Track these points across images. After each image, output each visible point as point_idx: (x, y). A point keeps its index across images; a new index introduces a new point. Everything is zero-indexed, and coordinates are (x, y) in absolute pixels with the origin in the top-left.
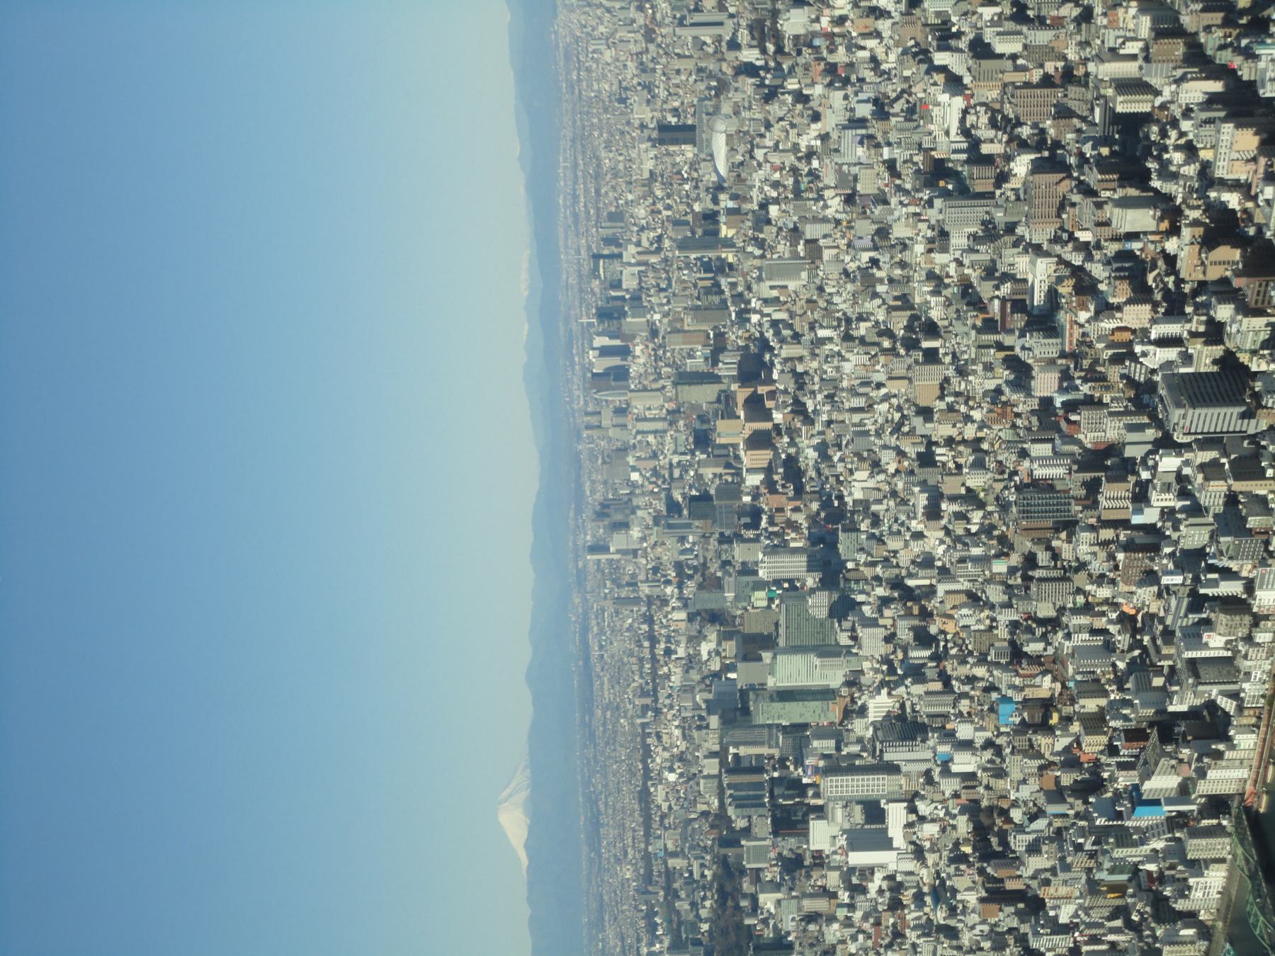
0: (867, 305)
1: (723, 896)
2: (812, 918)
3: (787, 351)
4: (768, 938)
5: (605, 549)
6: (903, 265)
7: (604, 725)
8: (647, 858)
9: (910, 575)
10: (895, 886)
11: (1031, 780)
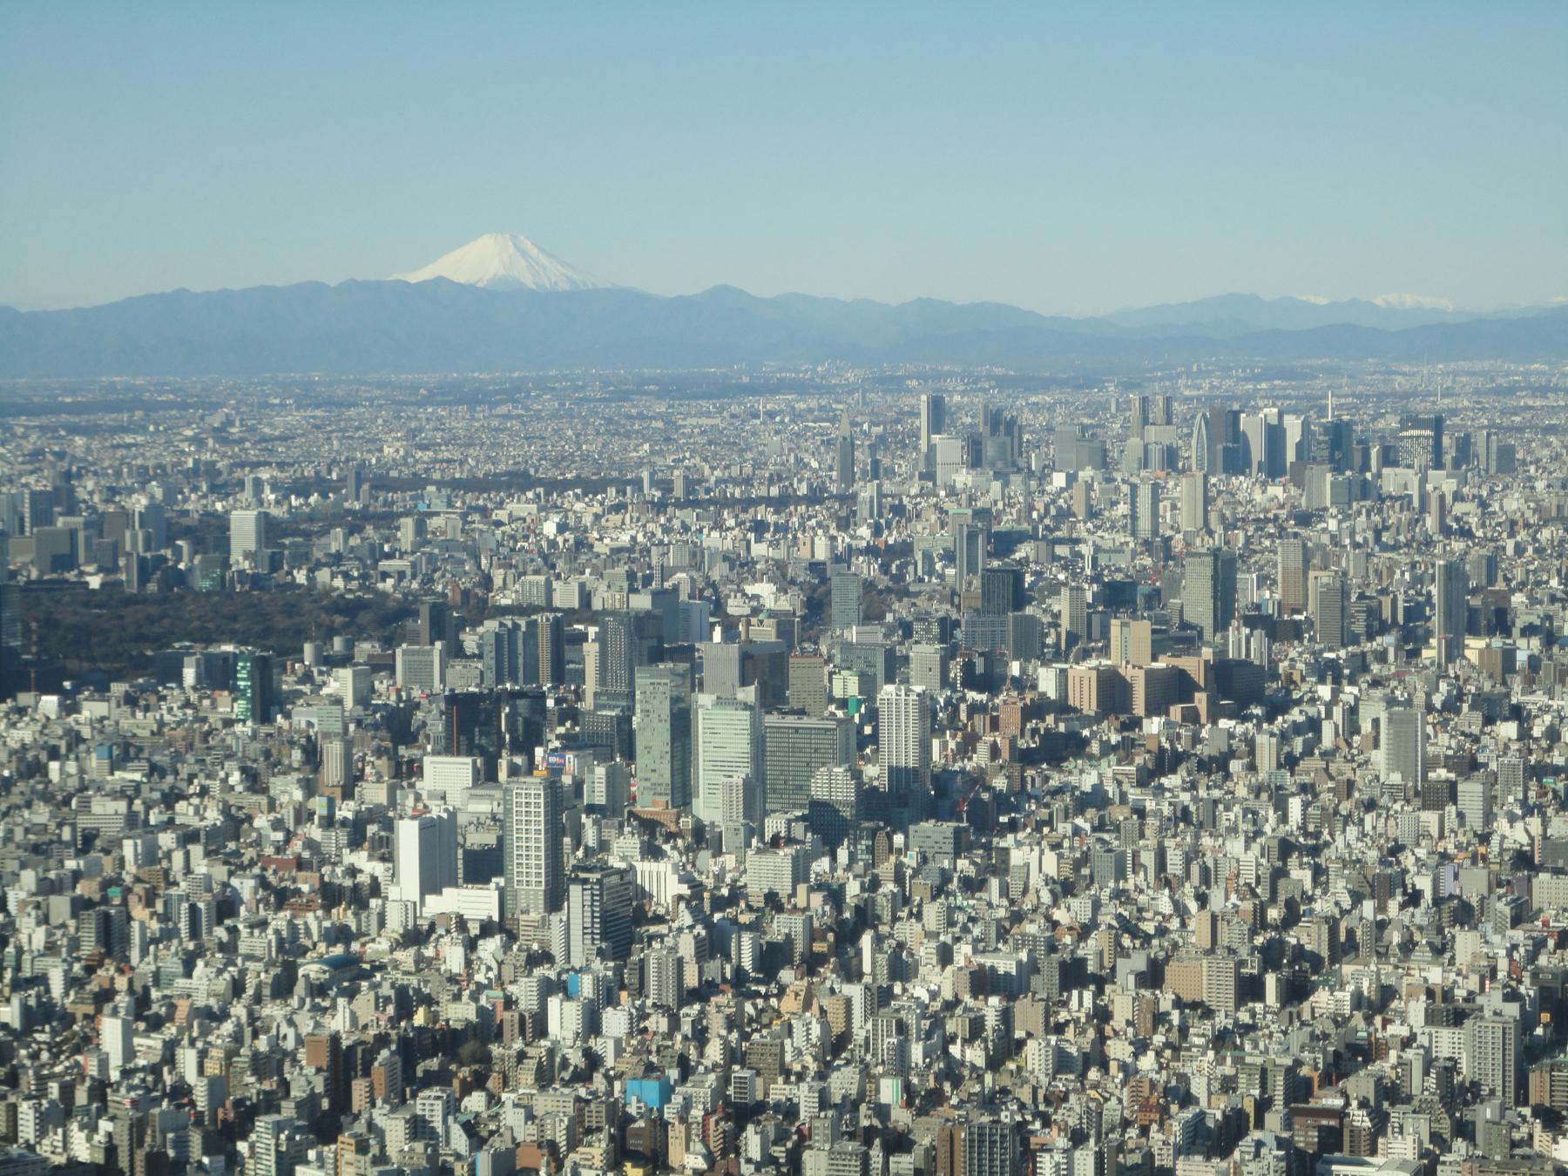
0: (1341, 884)
2: (313, 755)
3: (1266, 744)
4: (280, 682)
5: (936, 425)
6: (1408, 947)
7: (641, 417)
8: (417, 483)
9: (878, 940)
10: (361, 896)
11: (532, 1129)
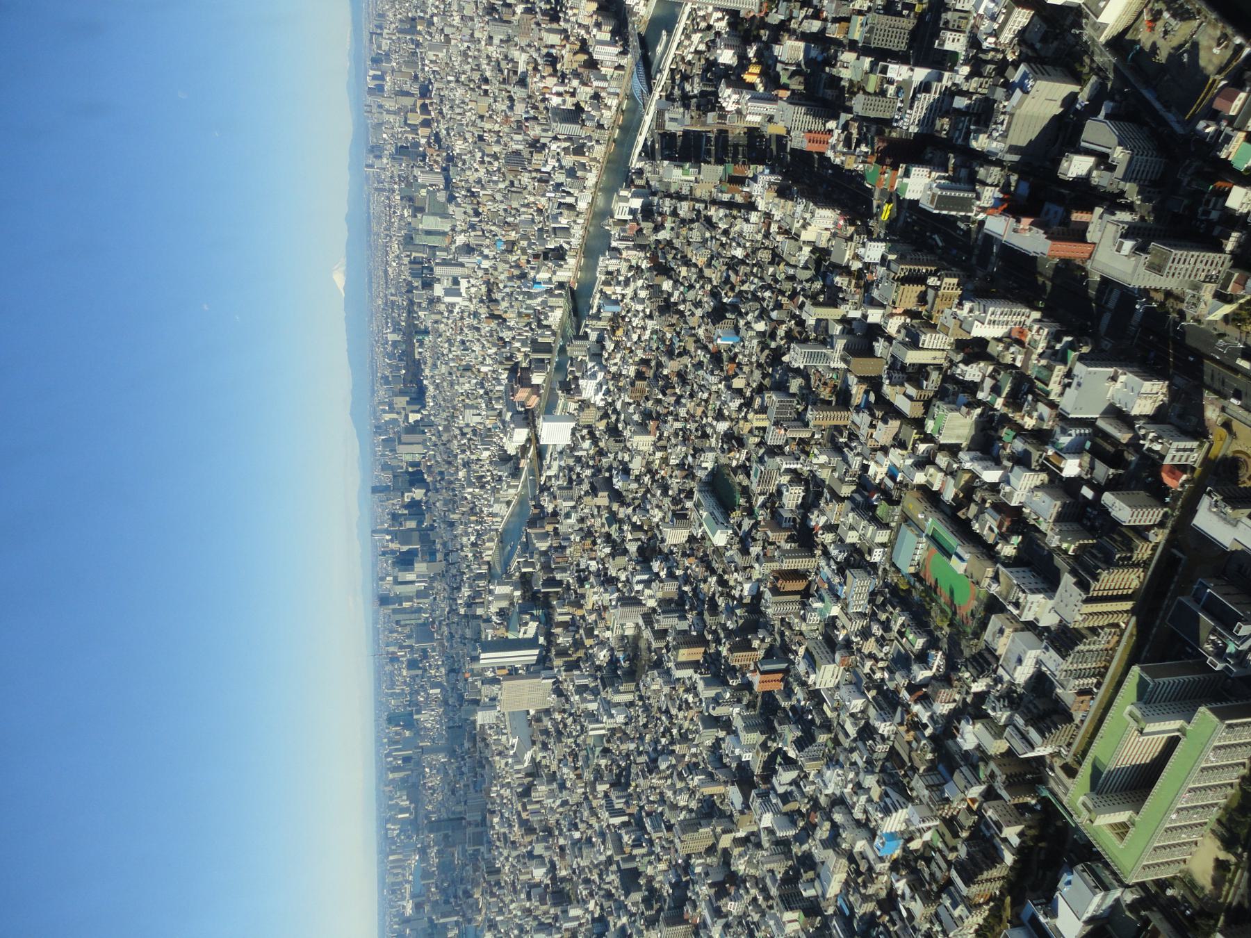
1: (410, 312)
2: (436, 322)
